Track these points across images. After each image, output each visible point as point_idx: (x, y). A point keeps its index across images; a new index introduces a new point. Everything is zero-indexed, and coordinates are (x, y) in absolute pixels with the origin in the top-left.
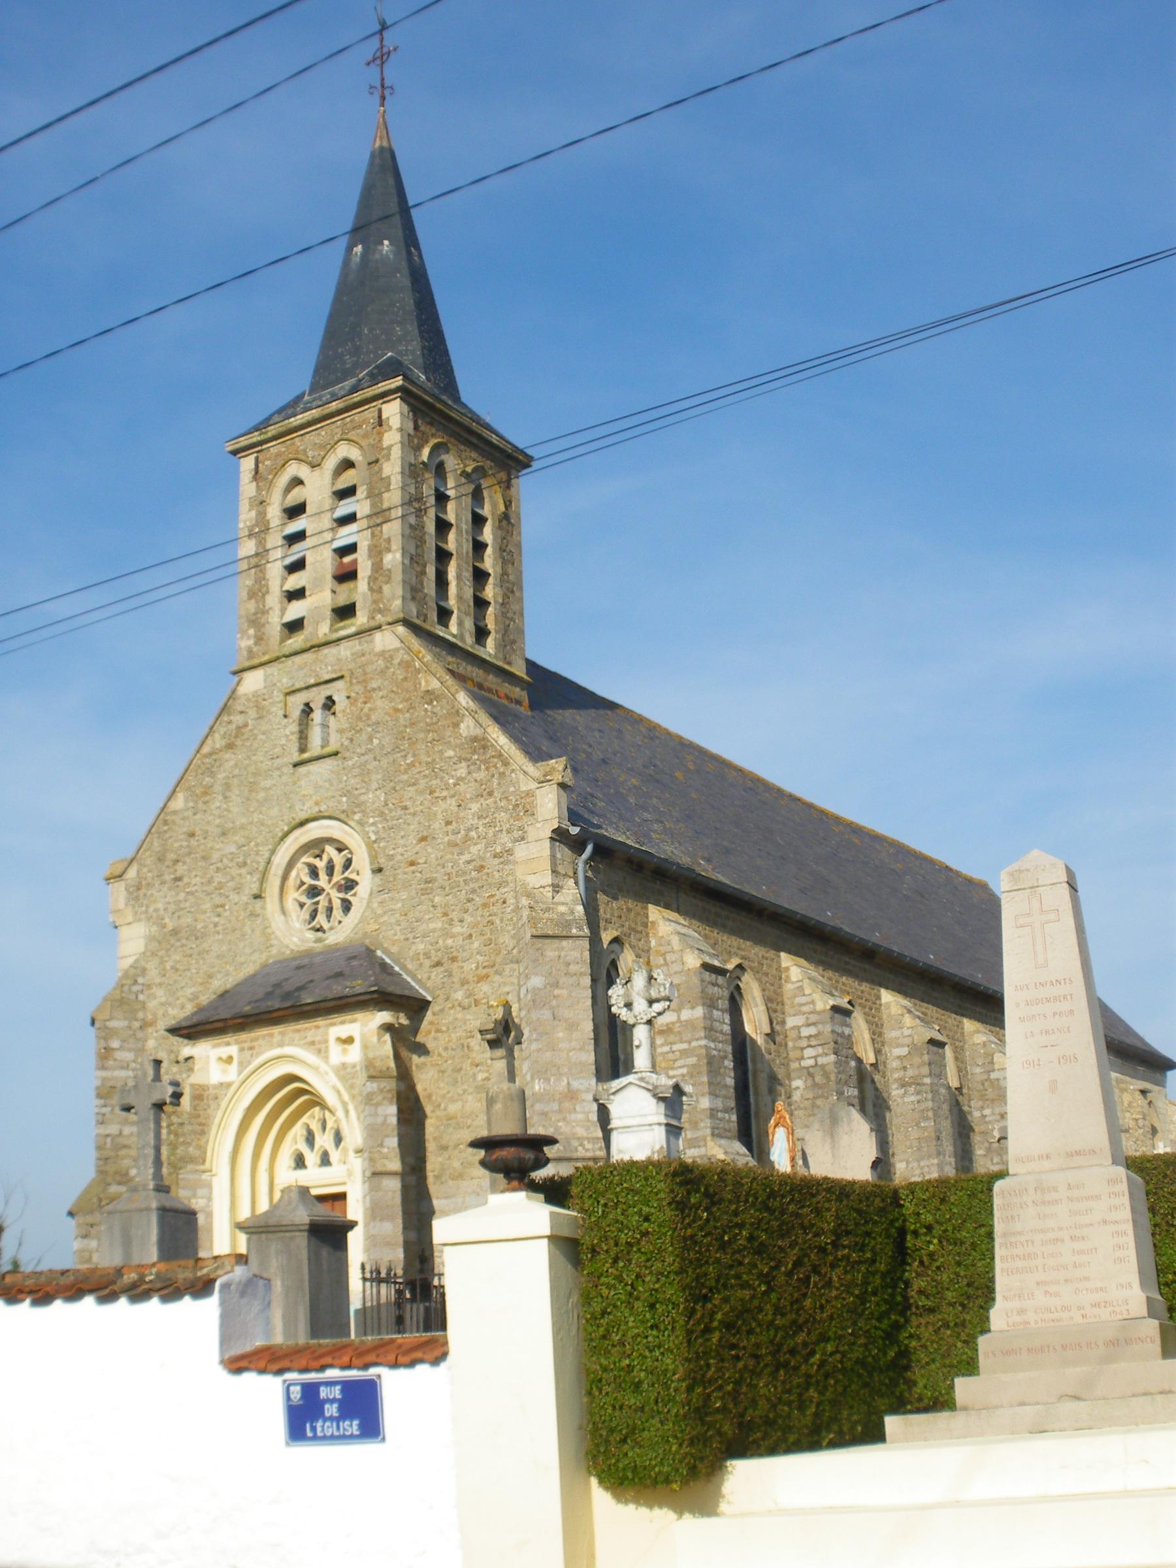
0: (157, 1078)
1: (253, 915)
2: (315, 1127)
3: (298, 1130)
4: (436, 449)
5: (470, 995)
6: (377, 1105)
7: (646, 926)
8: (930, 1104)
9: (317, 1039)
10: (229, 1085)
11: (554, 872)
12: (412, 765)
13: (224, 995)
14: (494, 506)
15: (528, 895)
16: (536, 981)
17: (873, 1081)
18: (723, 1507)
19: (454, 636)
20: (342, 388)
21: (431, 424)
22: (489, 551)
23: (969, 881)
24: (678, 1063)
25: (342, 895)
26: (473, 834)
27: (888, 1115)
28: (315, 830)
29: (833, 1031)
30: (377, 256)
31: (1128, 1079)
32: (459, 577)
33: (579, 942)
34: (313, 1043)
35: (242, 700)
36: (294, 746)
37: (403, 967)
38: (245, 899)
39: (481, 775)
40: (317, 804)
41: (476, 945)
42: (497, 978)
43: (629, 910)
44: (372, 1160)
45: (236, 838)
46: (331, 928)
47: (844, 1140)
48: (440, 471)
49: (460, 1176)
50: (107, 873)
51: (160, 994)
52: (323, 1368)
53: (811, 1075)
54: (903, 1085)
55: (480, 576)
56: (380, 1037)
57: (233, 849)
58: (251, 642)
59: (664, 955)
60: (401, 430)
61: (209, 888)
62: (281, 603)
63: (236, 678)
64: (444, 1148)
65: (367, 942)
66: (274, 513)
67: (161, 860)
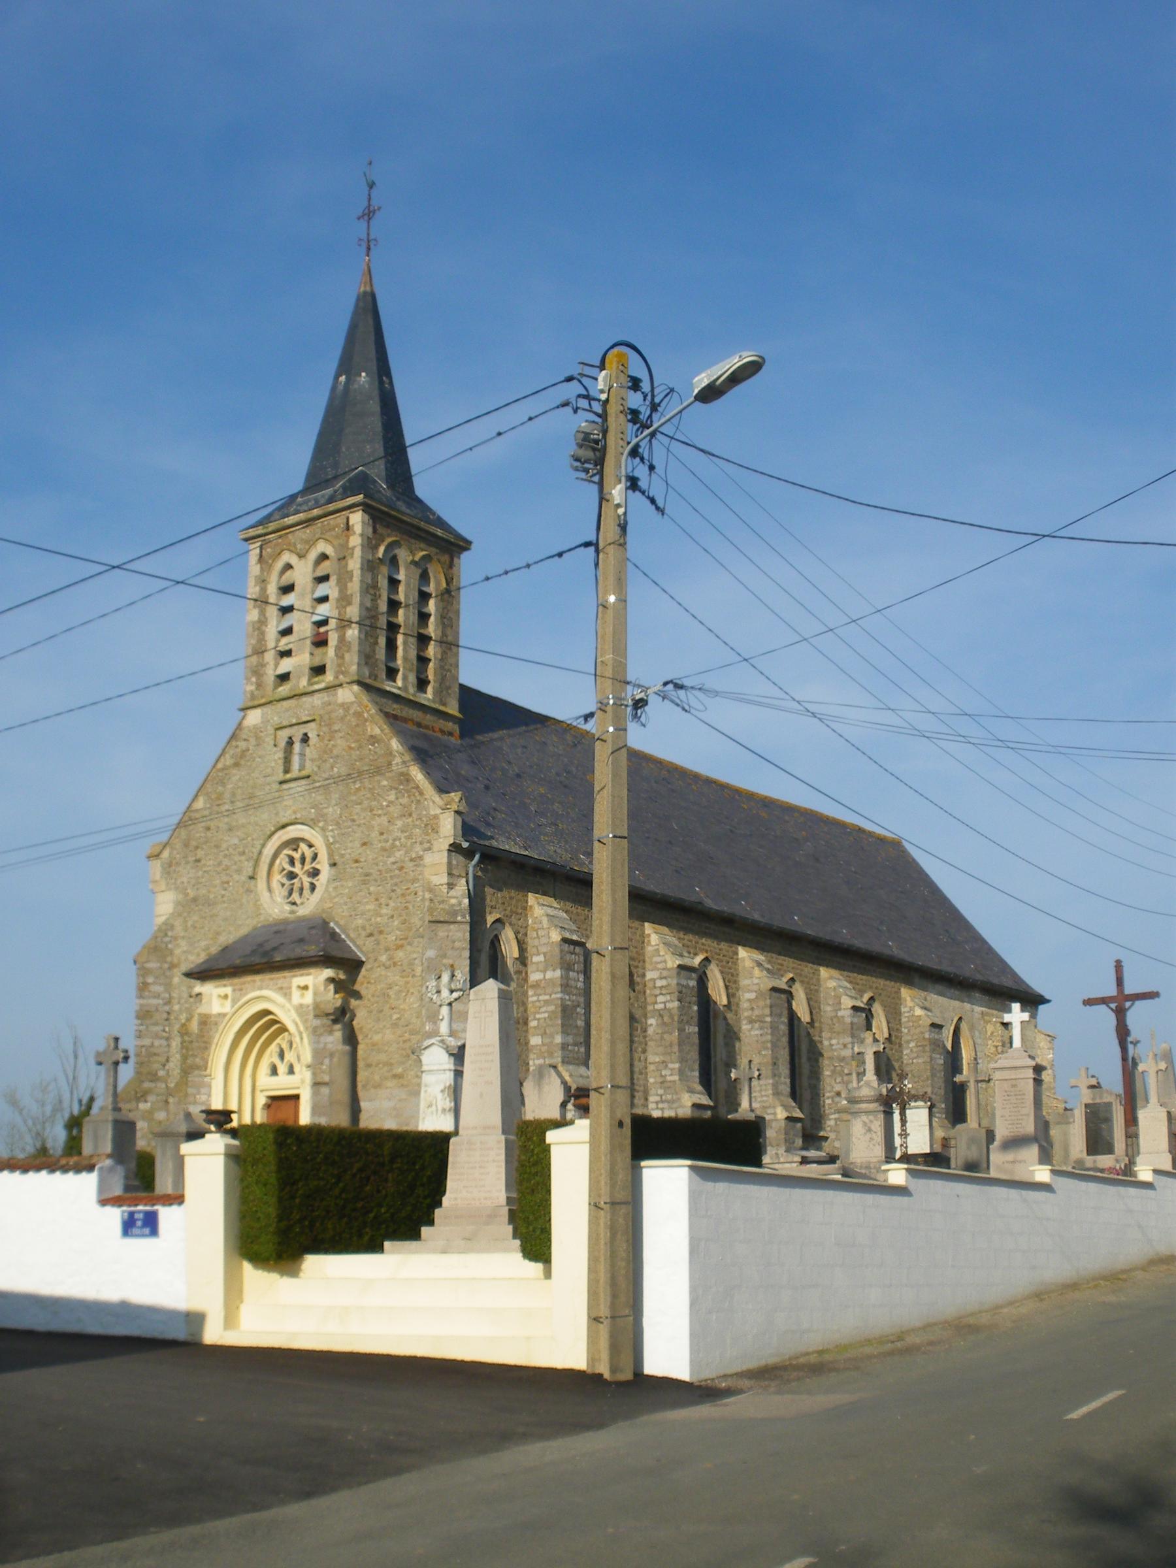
0: (116, 1047)
1: (249, 891)
2: (285, 1046)
3: (273, 1048)
4: (390, 547)
5: (390, 958)
6: (321, 1035)
7: (525, 908)
8: (769, 1037)
9: (285, 985)
10: (224, 1015)
11: (450, 874)
12: (358, 789)
13: (225, 949)
14: (438, 583)
15: (431, 890)
16: (431, 953)
17: (725, 1018)
18: (301, 1274)
19: (399, 688)
20: (323, 496)
21: (388, 527)
22: (432, 619)
23: (882, 840)
24: (543, 1010)
25: (310, 880)
26: (397, 843)
27: (737, 1044)
28: (293, 832)
29: (678, 984)
30: (356, 386)
31: (995, 1012)
32: (405, 643)
33: (462, 926)
34: (281, 988)
35: (246, 731)
36: (280, 769)
37: (348, 936)
38: (243, 878)
39: (405, 801)
40: (295, 812)
41: (396, 923)
42: (408, 948)
43: (511, 898)
44: (314, 1074)
45: (238, 833)
46: (302, 904)
47: (546, 1088)
48: (394, 562)
49: (378, 1086)
50: (148, 852)
51: (183, 944)
52: (136, 1205)
53: (661, 1016)
54: (751, 1021)
55: (423, 640)
56: (326, 987)
57: (236, 841)
58: (253, 688)
59: (537, 931)
60: (362, 535)
61: (219, 869)
62: (275, 659)
63: (242, 714)
64: (369, 1066)
65: (324, 916)
66: (272, 589)
67: (186, 845)
